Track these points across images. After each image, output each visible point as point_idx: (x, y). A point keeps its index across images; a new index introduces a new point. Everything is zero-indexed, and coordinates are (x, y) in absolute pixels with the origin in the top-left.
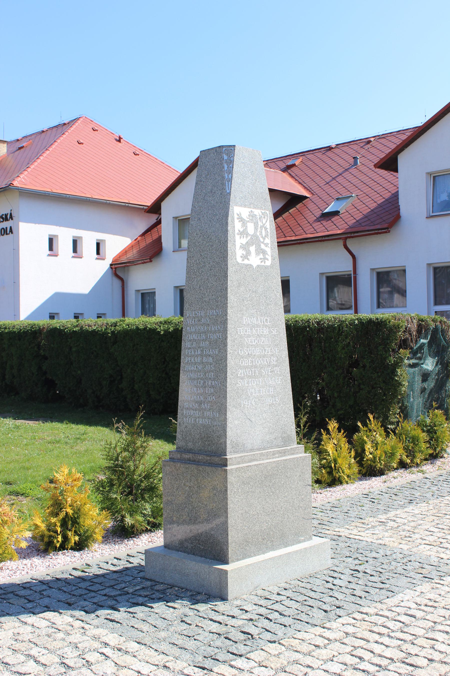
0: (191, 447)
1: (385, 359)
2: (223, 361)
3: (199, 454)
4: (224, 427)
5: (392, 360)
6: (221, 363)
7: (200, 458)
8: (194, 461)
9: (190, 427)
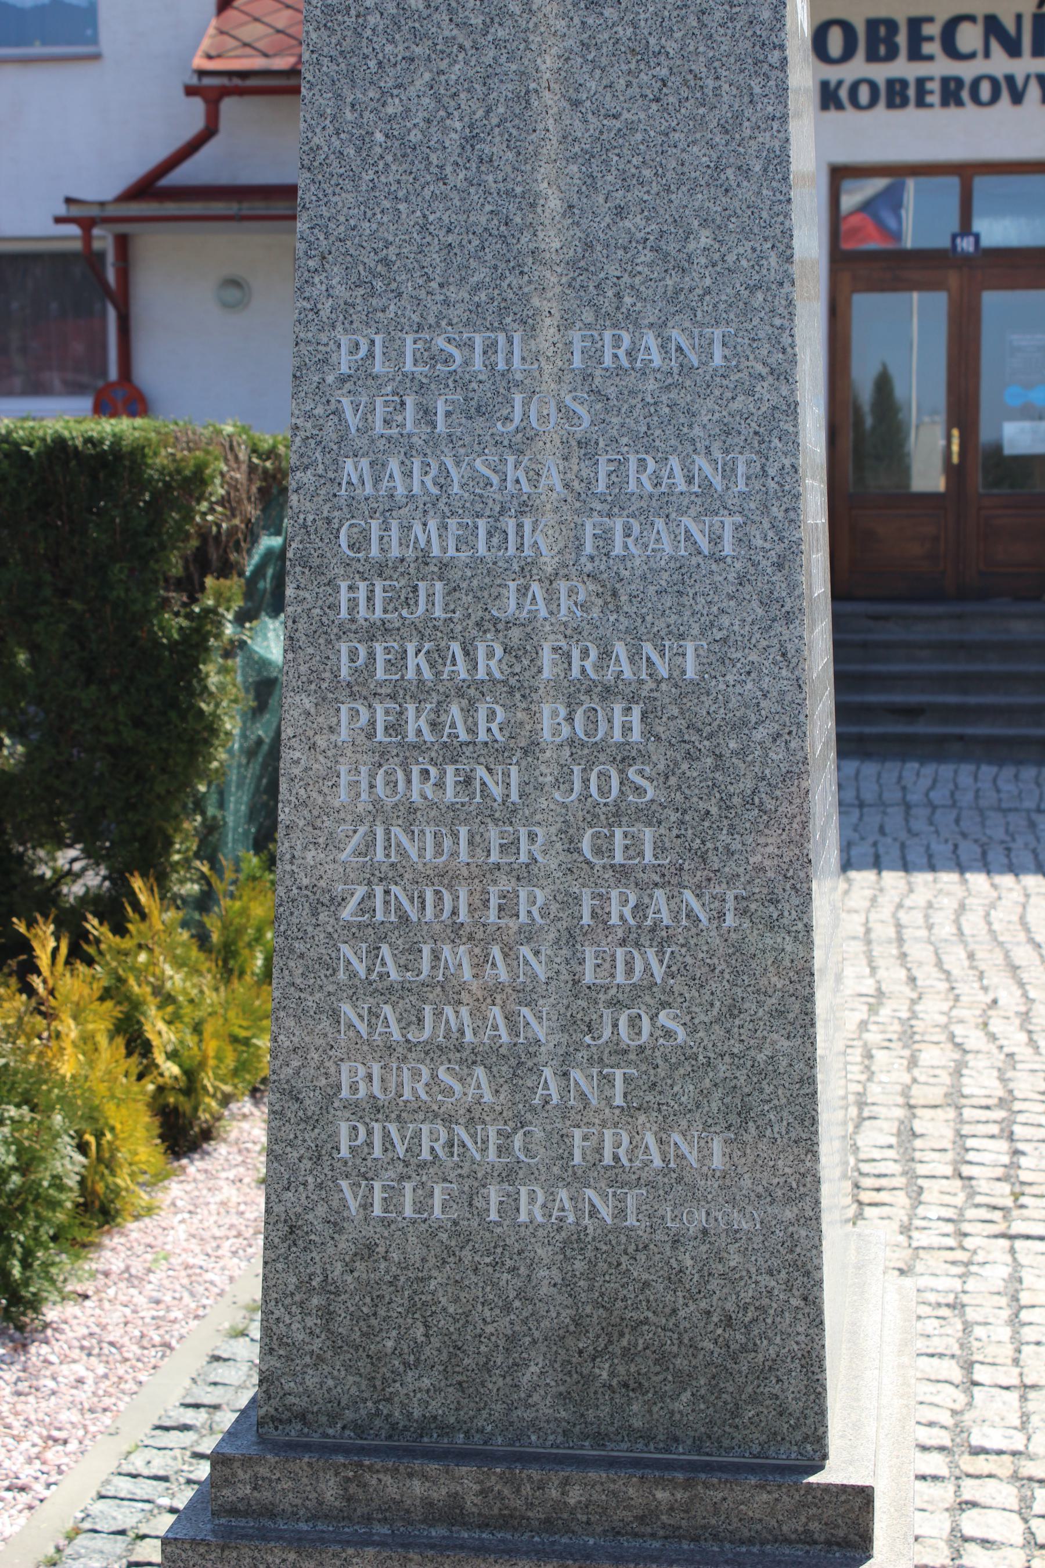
0: (435, 1406)
1: (146, 615)
2: (758, 735)
3: (561, 1461)
4: (792, 1243)
5: (173, 623)
6: (742, 753)
7: (575, 1496)
8: (507, 1521)
9: (416, 1254)
